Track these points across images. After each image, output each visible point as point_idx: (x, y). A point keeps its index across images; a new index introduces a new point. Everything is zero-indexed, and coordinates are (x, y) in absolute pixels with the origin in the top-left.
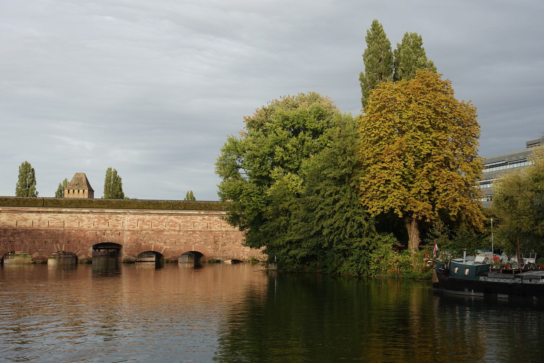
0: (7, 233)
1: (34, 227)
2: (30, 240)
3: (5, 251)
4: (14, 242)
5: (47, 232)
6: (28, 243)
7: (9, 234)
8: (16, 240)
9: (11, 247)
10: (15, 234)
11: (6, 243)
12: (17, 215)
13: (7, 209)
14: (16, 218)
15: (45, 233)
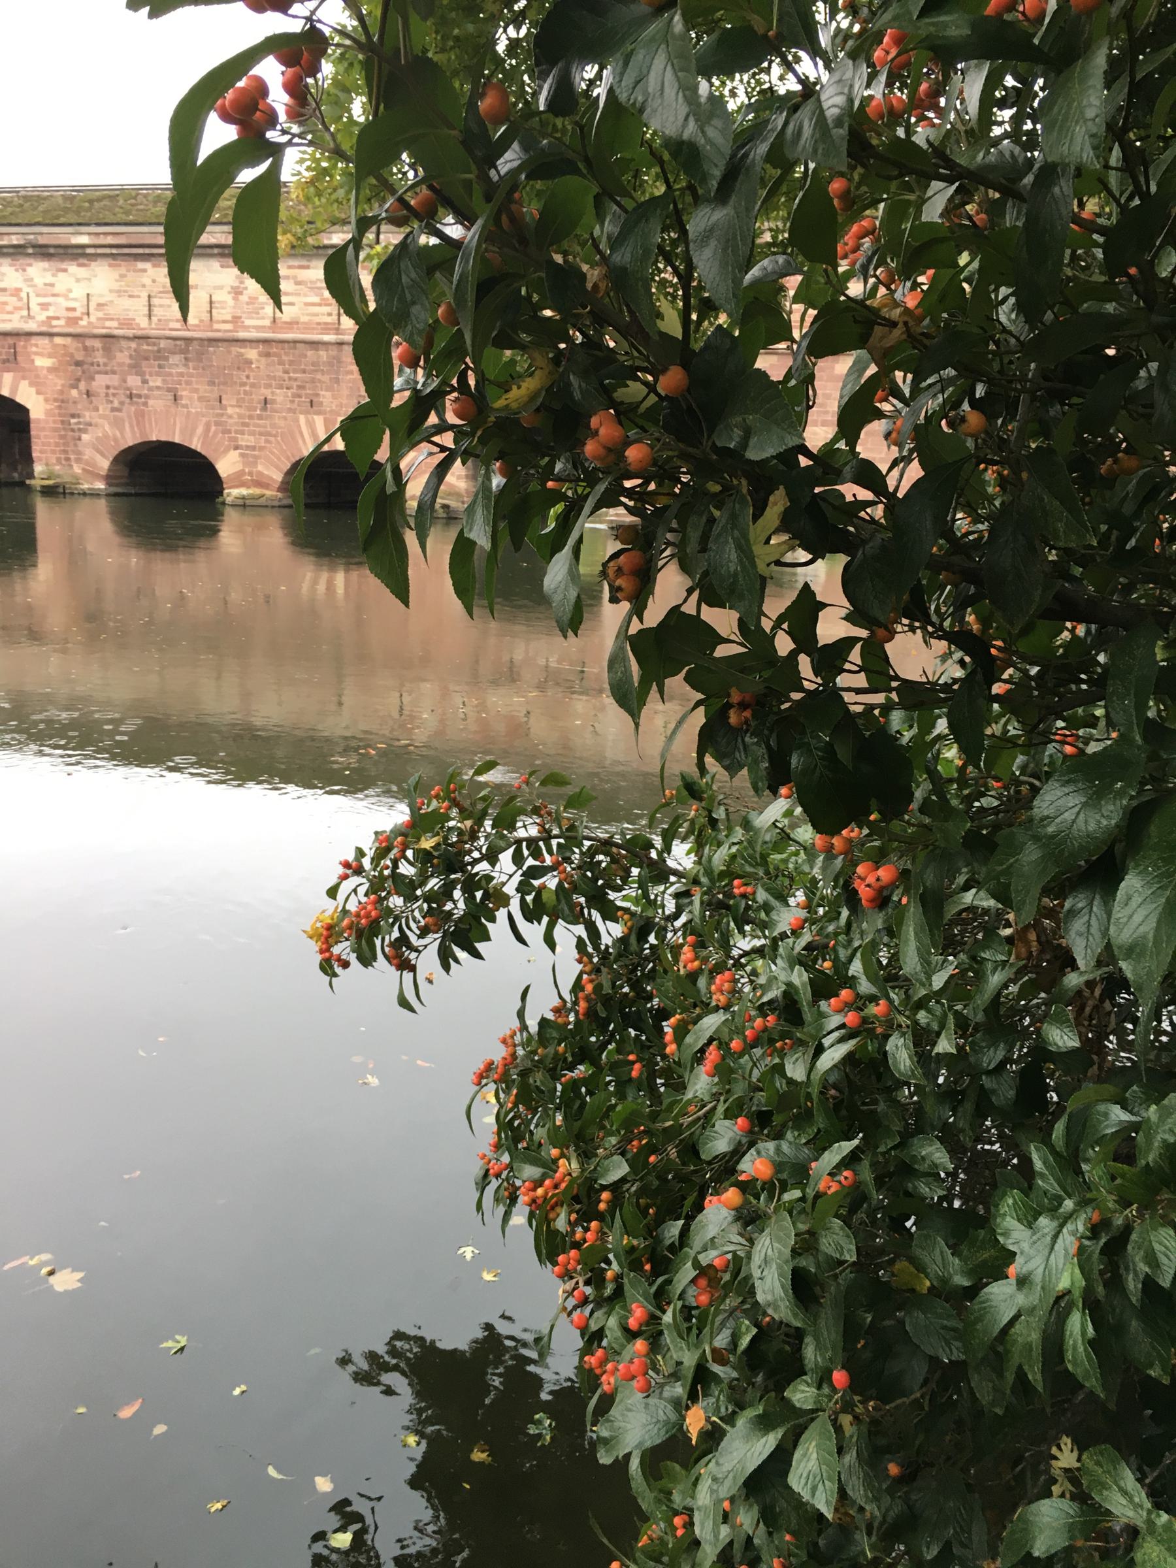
0: (118, 354)
1: (216, 326)
2: (204, 388)
3: (116, 440)
4: (147, 397)
5: (268, 355)
6: (196, 408)
7: (123, 357)
8: (150, 389)
9: (138, 423)
10: (147, 359)
11: (116, 404)
12: (147, 265)
13: (109, 236)
14: (146, 281)
15: (263, 360)
